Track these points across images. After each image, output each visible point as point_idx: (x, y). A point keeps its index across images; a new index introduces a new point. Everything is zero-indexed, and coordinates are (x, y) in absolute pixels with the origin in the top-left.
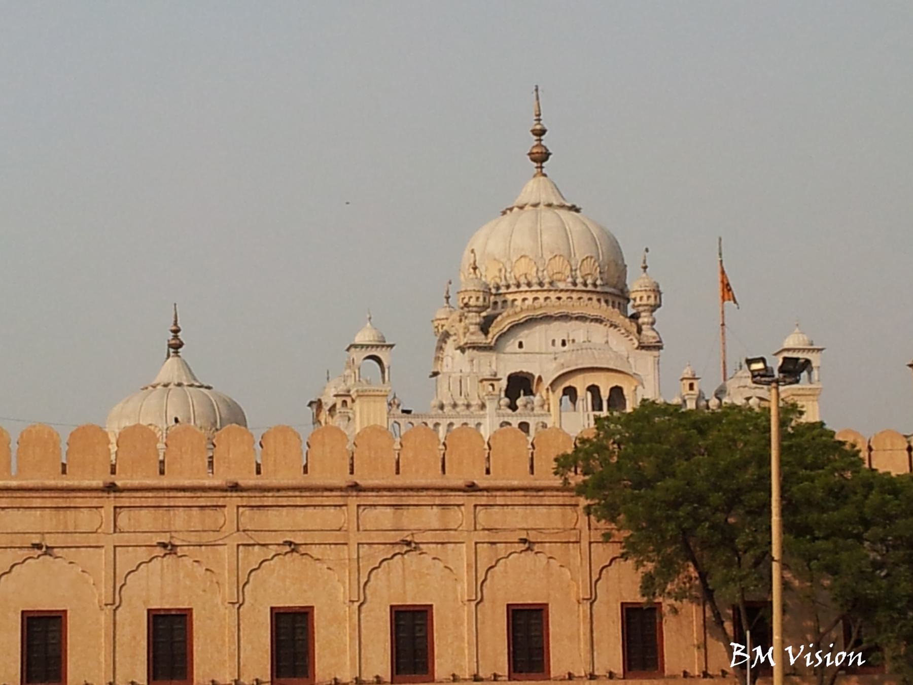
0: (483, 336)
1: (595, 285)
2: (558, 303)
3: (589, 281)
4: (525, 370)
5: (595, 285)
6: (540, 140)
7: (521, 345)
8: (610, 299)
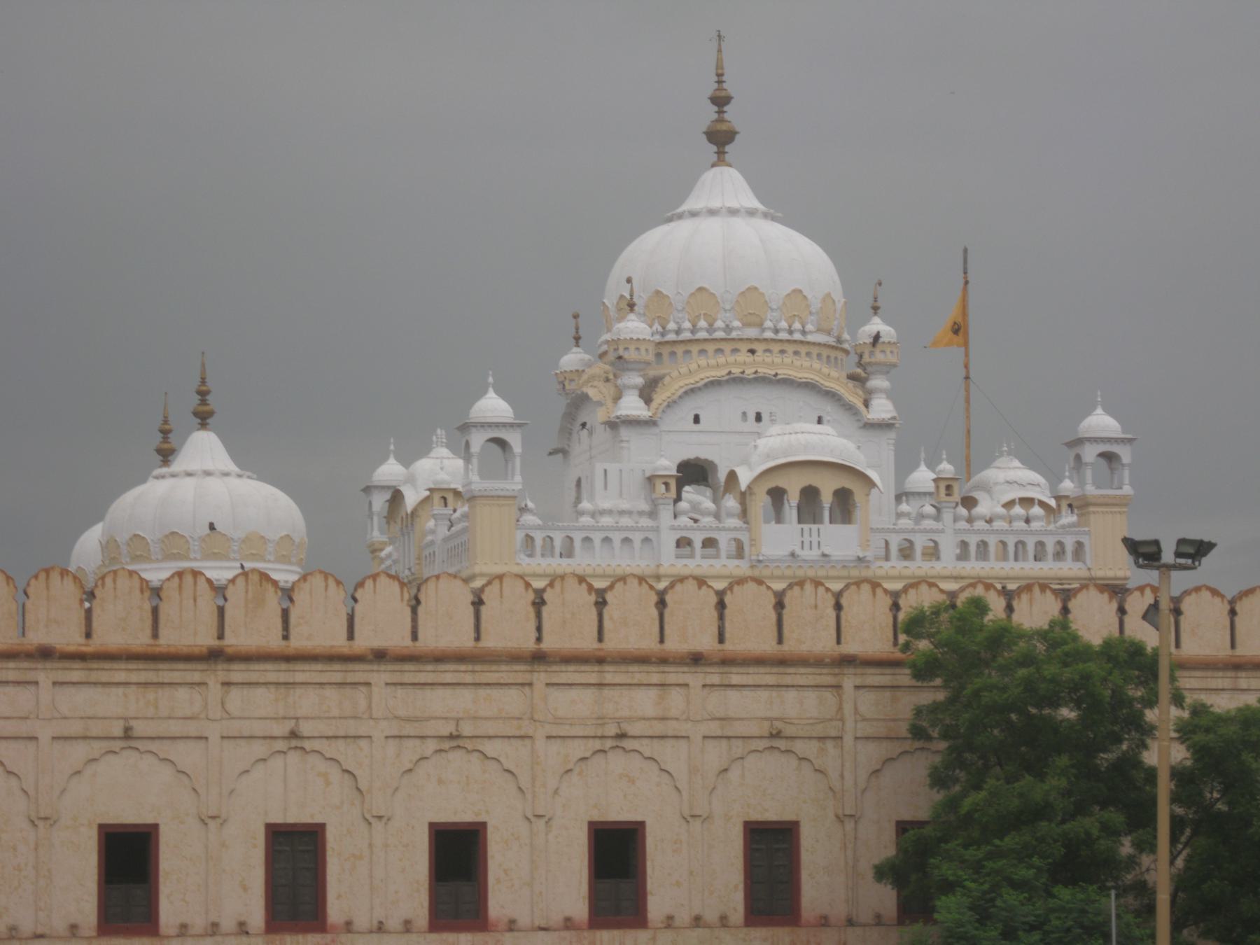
0: (641, 404)
1: (804, 333)
2: (749, 358)
3: (797, 326)
4: (703, 456)
5: (804, 333)
6: (720, 112)
7: (697, 419)
8: (825, 352)
